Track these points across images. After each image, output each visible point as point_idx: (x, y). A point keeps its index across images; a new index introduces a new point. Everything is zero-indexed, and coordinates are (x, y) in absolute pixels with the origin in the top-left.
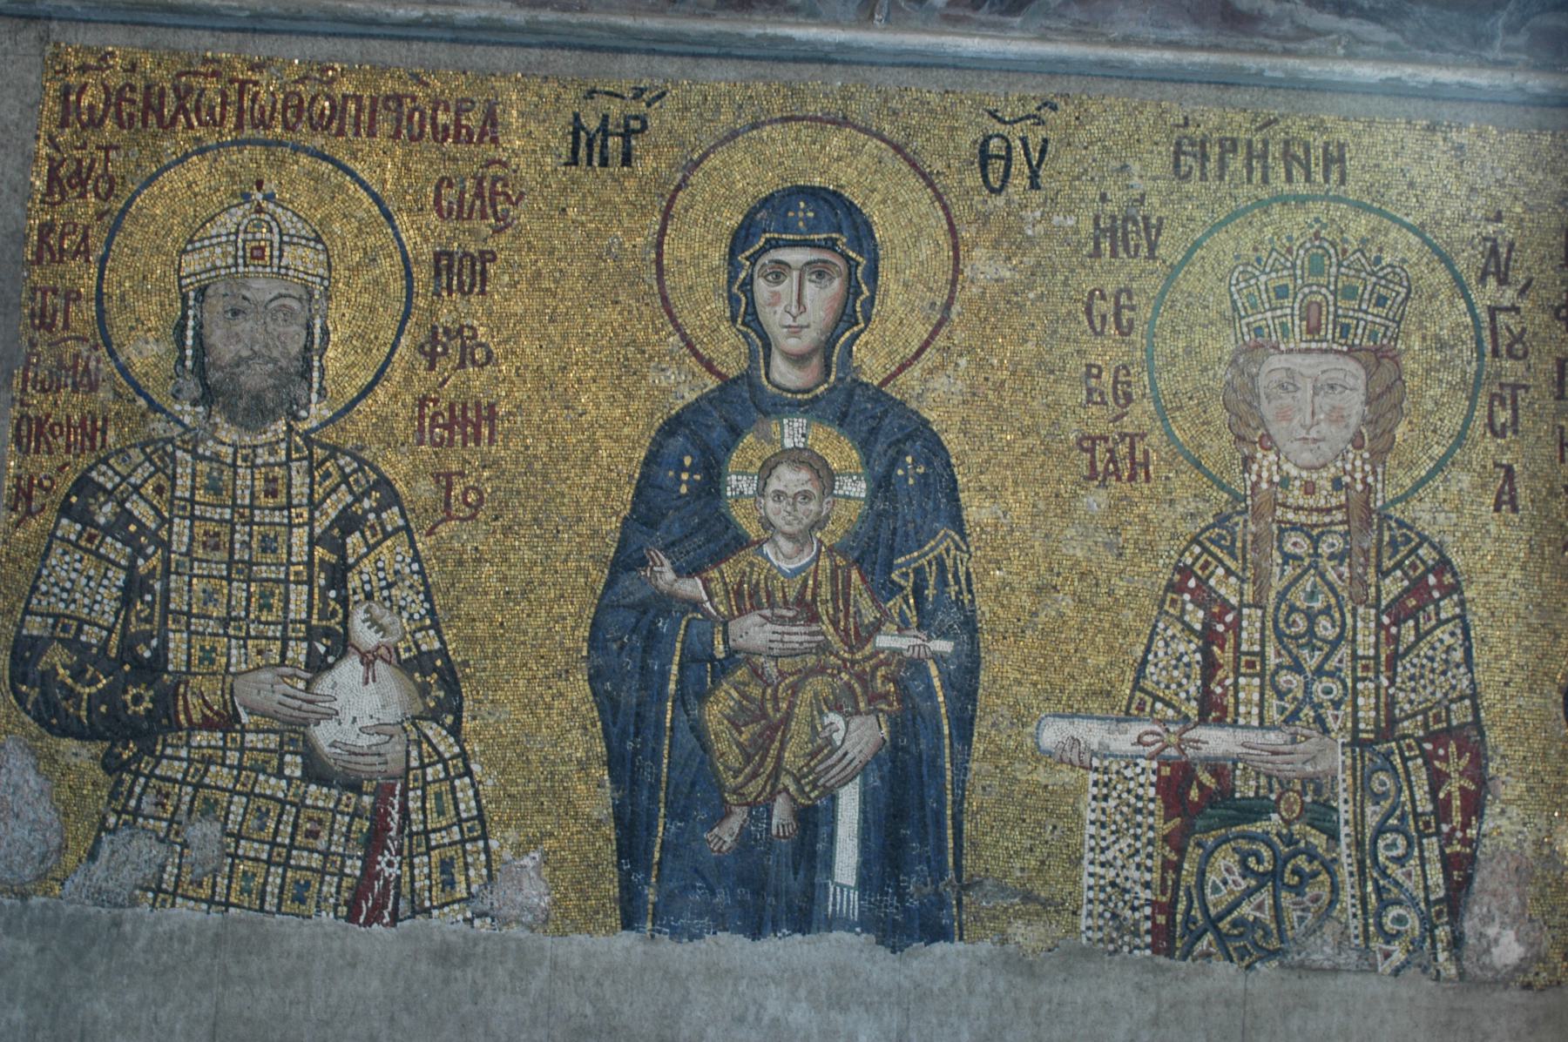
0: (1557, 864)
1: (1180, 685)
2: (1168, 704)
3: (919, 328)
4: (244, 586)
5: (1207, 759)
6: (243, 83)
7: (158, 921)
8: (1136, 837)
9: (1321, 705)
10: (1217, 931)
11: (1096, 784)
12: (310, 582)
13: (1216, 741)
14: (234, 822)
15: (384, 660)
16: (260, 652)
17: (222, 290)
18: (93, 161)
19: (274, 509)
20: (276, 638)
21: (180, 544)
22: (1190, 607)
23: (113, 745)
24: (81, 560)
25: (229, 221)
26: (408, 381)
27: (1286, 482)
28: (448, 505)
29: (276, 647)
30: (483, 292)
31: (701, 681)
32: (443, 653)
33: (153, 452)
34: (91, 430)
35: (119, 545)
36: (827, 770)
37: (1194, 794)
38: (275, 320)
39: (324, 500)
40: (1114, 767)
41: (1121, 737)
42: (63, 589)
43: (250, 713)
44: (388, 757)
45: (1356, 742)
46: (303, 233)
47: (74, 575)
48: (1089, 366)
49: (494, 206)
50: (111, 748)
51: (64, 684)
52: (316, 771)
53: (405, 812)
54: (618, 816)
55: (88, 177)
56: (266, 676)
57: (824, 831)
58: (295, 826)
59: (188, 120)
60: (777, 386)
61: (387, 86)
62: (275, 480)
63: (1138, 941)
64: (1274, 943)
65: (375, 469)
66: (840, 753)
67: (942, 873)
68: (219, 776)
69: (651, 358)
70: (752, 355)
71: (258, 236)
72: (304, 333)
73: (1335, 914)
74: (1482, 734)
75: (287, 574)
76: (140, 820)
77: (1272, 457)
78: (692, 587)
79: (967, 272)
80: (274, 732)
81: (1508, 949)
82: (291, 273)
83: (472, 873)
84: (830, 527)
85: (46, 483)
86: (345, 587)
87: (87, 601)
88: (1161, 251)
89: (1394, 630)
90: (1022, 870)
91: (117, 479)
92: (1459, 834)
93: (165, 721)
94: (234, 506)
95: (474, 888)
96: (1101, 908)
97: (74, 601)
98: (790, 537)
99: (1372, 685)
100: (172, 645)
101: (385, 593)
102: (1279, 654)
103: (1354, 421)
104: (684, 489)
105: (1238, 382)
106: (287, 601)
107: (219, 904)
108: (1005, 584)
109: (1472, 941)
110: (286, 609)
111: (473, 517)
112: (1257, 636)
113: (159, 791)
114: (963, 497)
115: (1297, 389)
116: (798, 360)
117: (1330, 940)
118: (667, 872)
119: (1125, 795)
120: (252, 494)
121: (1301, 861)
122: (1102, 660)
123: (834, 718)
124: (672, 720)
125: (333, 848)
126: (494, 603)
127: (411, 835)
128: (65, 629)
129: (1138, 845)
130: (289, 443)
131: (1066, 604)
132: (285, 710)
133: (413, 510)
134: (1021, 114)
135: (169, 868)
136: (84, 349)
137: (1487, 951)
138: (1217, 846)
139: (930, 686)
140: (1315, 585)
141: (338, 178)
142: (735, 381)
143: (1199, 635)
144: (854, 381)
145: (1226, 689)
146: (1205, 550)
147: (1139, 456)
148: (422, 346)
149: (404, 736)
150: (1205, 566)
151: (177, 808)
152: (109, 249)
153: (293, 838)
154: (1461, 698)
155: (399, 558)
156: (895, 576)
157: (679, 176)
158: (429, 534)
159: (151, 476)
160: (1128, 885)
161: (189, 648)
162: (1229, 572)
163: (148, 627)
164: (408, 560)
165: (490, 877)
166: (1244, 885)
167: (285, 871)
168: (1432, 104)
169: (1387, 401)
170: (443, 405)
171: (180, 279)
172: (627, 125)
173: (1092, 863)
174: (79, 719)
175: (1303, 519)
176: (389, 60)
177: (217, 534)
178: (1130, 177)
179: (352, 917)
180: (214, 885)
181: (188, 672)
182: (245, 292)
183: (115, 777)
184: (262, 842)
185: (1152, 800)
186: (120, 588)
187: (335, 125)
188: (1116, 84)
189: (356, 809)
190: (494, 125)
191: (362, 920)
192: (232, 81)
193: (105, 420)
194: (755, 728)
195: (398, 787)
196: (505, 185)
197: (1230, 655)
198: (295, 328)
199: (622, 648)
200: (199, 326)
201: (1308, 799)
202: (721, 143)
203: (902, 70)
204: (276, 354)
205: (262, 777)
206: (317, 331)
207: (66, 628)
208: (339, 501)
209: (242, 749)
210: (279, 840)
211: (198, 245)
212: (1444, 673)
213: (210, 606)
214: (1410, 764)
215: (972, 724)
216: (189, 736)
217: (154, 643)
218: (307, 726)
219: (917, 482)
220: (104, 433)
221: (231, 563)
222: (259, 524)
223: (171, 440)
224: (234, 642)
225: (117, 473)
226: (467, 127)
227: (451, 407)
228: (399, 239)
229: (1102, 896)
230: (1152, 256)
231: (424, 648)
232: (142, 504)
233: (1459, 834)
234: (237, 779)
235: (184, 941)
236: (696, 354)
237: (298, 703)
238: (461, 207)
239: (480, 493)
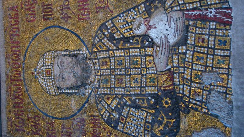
4: (132, 70)
6: (11, 79)
7: (236, 93)
12: (129, 49)
14: (202, 68)
17: (57, 83)
18: (32, 122)
19: (110, 62)
20: (145, 59)
24: (129, 123)
25: (41, 81)
28: (104, 7)
29: (148, 58)
33: (99, 101)
34: (95, 120)
35: (124, 110)
39: (107, 47)
42: (137, 128)
43: (168, 66)
44: (177, 17)
46: (42, 60)
47: (133, 125)
49: (31, 5)
51: (164, 128)
52: (183, 41)
53: (194, 9)
55: (35, 123)
56: (156, 61)
58: (201, 47)
59: (20, 95)
61: (8, 39)
62: (103, 63)
65: (97, 32)
71: (44, 73)
72: (66, 57)
75: (127, 56)
76: (204, 100)
80: (172, 57)
82: (52, 62)
85: (109, 134)
86: (129, 37)
87: (140, 120)
93: (172, 94)
94: (111, 75)
97: (140, 124)
100: (150, 92)
101: (130, 24)
106: (135, 56)
107: (229, 71)
110: (137, 56)
120: (107, 69)
125: (207, 33)
127: (201, 6)
128: (148, 127)
130: (93, 59)
132: (166, 53)
133: (107, 18)
135: (219, 90)
136: (75, 123)
148: (66, 21)
149: (171, 13)
151: (199, 88)
152: (51, 116)
155: (120, 21)
158: (112, 12)
159: (105, 101)
161: (150, 86)
163: (145, 100)
167: (216, 49)
171: (56, 95)
174: (174, 122)
176: (3, 39)
177: (118, 79)
179: (229, 24)
180: (223, 74)
181: (157, 86)
182: (58, 75)
183: (191, 110)
184: (207, 58)
186: (136, 110)
189: (194, 26)
191: (230, 20)
192: (11, 83)
195: (186, 12)
204: (72, 65)
205: (187, 60)
206: (65, 53)
207: (148, 127)
208: (106, 42)
209: (179, 67)
210: (206, 52)
211: (48, 90)
213: (138, 80)
216: (176, 85)
217: (150, 98)
218: (170, 46)
220: (95, 116)
221: (126, 75)
222: (115, 66)
223: (95, 95)
224: (148, 72)
225: (105, 112)
226: (15, 15)
227: (80, 10)
228: (42, 31)
232: (113, 104)
234: (188, 68)
235: (242, 83)
237: (163, 49)
238: (32, 14)
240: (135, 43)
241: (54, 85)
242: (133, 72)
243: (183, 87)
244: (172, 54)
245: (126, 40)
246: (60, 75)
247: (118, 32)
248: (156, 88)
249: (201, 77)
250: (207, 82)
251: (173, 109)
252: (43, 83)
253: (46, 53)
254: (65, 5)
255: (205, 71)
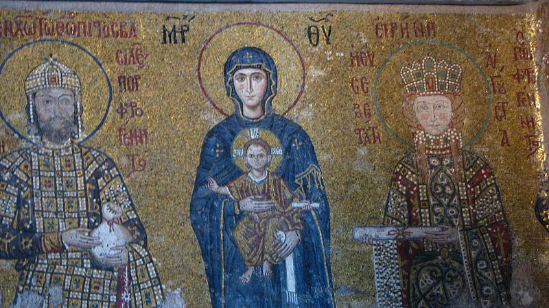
0: (540, 267)
1: (400, 213)
2: (397, 220)
3: (294, 94)
5: (414, 238)
6: (42, 19)
8: (392, 268)
9: (451, 217)
10: (425, 299)
11: (375, 250)
12: (86, 196)
13: (416, 232)
15: (116, 223)
16: (70, 223)
17: (42, 94)
21: (36, 185)
22: (400, 186)
23: (18, 261)
26: (113, 122)
27: (428, 141)
28: (133, 166)
30: (137, 89)
31: (232, 222)
32: (138, 219)
36: (281, 251)
37: (410, 251)
38: (62, 103)
39: (88, 167)
40: (381, 244)
41: (383, 233)
43: (69, 245)
45: (464, 229)
48: (355, 105)
49: (138, 59)
50: (18, 261)
52: (96, 265)
53: (130, 277)
54: (208, 274)
56: (73, 232)
57: (282, 273)
58: (90, 285)
60: (246, 117)
61: (95, 18)
62: (69, 161)
63: (398, 304)
64: (445, 302)
65: (105, 155)
66: (285, 245)
67: (326, 284)
68: (60, 269)
69: (200, 110)
70: (236, 107)
73: (465, 290)
74: (507, 223)
76: (32, 288)
77: (422, 132)
78: (225, 190)
79: (309, 74)
81: (528, 299)
83: (157, 297)
84: (271, 165)
86: (99, 198)
88: (375, 63)
89: (472, 189)
90: (354, 282)
91: (10, 164)
92: (505, 259)
93: (37, 251)
95: (158, 303)
96: (383, 294)
98: (257, 170)
99: (467, 209)
100: (37, 223)
101: (114, 199)
102: (434, 200)
103: (449, 118)
104: (218, 155)
105: (407, 107)
108: (335, 182)
109: (514, 297)
111: (143, 169)
112: (425, 194)
113: (38, 276)
114: (317, 152)
115: (428, 108)
116: (253, 108)
117: (465, 299)
118: (227, 292)
119: (386, 253)
120: (61, 167)
121: (451, 272)
122: (372, 207)
123: (281, 233)
124: (223, 237)
126: (154, 200)
127: (133, 285)
129: (393, 270)
131: (357, 187)
134: (320, 18)
135: (44, 304)
137: (520, 300)
138: (421, 269)
139: (313, 220)
140: (443, 175)
141: (81, 51)
142: (231, 116)
143: (405, 195)
144: (274, 114)
145: (417, 214)
146: (403, 166)
147: (376, 134)
148: (118, 110)
150: (404, 172)
151: (45, 282)
153: (90, 289)
154: (499, 212)
156: (296, 181)
157: (203, 46)
158: (128, 176)
160: (392, 285)
161: (44, 223)
162: (413, 173)
163: (27, 217)
164: (121, 186)
165: (163, 298)
166: (432, 282)
168: (462, 7)
169: (460, 111)
170: (128, 130)
171: (25, 91)
172: (182, 29)
173: (378, 278)
174: (5, 252)
175: (436, 153)
177: (50, 182)
178: (361, 38)
182: (50, 94)
185: (396, 254)
187: (77, 33)
188: (353, 6)
190: (134, 31)
193: (3, 142)
194: (254, 238)
196: (141, 52)
197: (416, 202)
198: (70, 106)
199: (202, 213)
200: (34, 107)
201: (451, 250)
202: (217, 33)
203: (278, 5)
204: (64, 116)
205: (76, 268)
206: (78, 107)
208: (93, 167)
212: (492, 203)
213: (50, 208)
214: (484, 236)
215: (329, 232)
216: (47, 256)
217: (31, 222)
218: (91, 248)
219: (300, 149)
220: (3, 147)
221: (56, 191)
223: (29, 149)
225: (9, 161)
227: (131, 131)
228: (105, 73)
229: (383, 289)
230: (372, 64)
231: (131, 217)
232: (20, 172)
233: (505, 259)
236: (216, 108)
237: (86, 241)
238: (126, 60)
239: (145, 161)
240: (93, 205)
241: (38, 88)
242: (60, 201)
243: (45, 264)
244: (81, 252)
245: (96, 193)
246: (51, 98)
247: (105, 184)
248: (42, 231)
249: (58, 284)
250: (52, 291)
251: (19, 251)
252: (40, 70)
253: (78, 77)
254: (136, 110)
255: (63, 289)
